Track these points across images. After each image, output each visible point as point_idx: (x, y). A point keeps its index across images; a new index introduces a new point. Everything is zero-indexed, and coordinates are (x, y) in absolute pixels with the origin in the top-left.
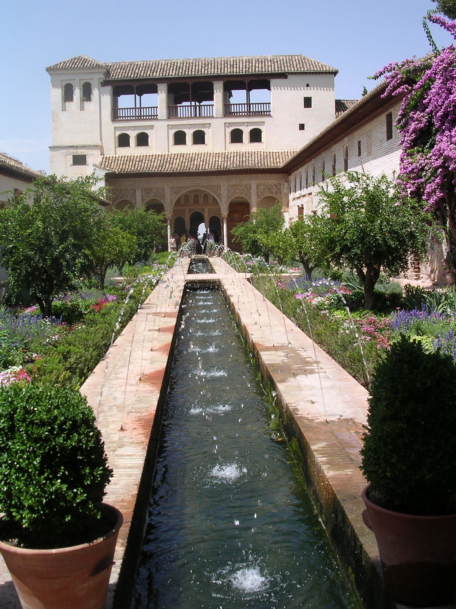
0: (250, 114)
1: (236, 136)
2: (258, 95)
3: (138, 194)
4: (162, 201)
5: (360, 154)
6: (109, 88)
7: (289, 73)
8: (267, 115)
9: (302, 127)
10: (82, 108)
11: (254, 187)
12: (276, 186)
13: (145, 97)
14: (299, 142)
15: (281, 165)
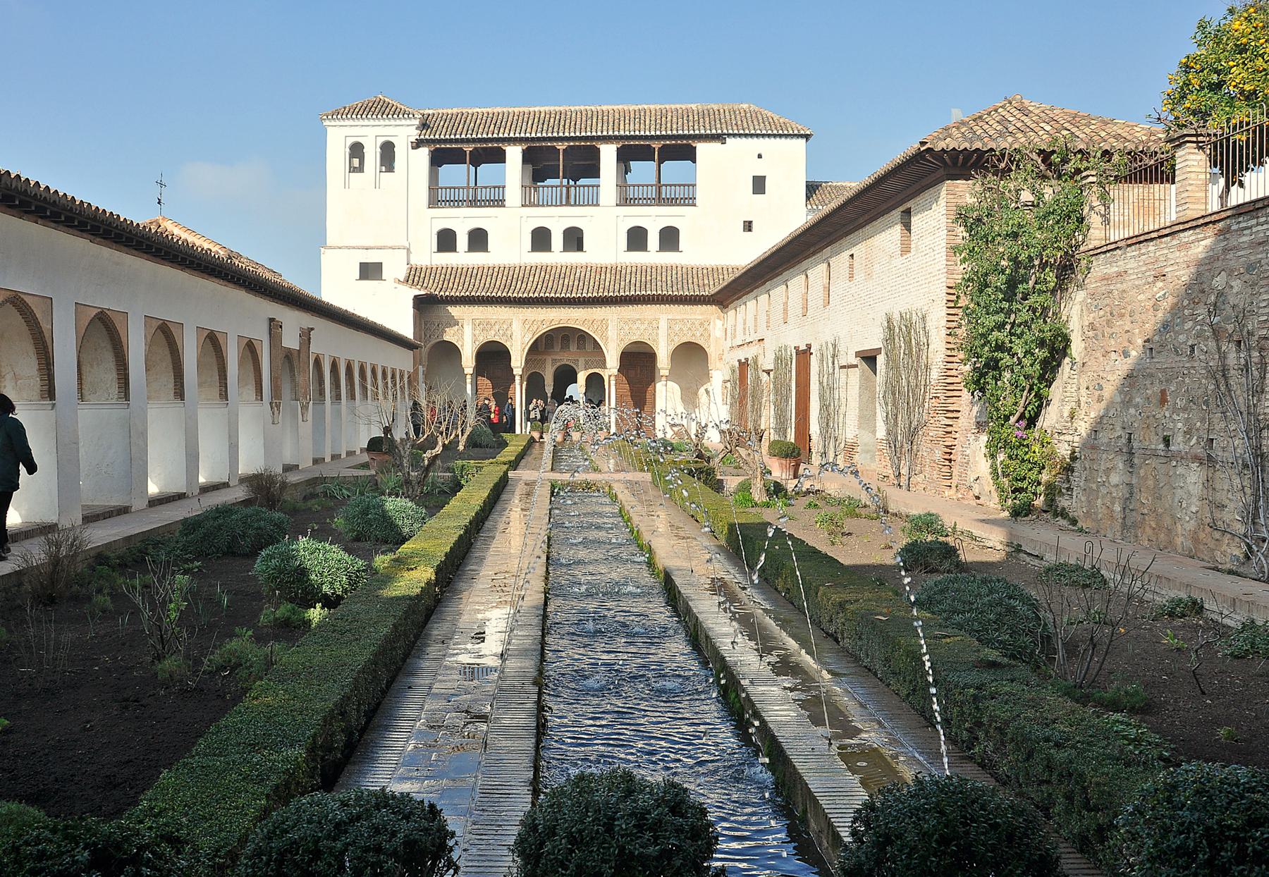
0: (660, 201)
1: (637, 239)
2: (673, 170)
3: (468, 330)
4: (508, 345)
5: (851, 277)
6: (424, 152)
7: (729, 135)
8: (688, 205)
9: (748, 226)
10: (377, 185)
11: (663, 325)
12: (701, 324)
13: (484, 168)
14: (746, 253)
15: (713, 290)
